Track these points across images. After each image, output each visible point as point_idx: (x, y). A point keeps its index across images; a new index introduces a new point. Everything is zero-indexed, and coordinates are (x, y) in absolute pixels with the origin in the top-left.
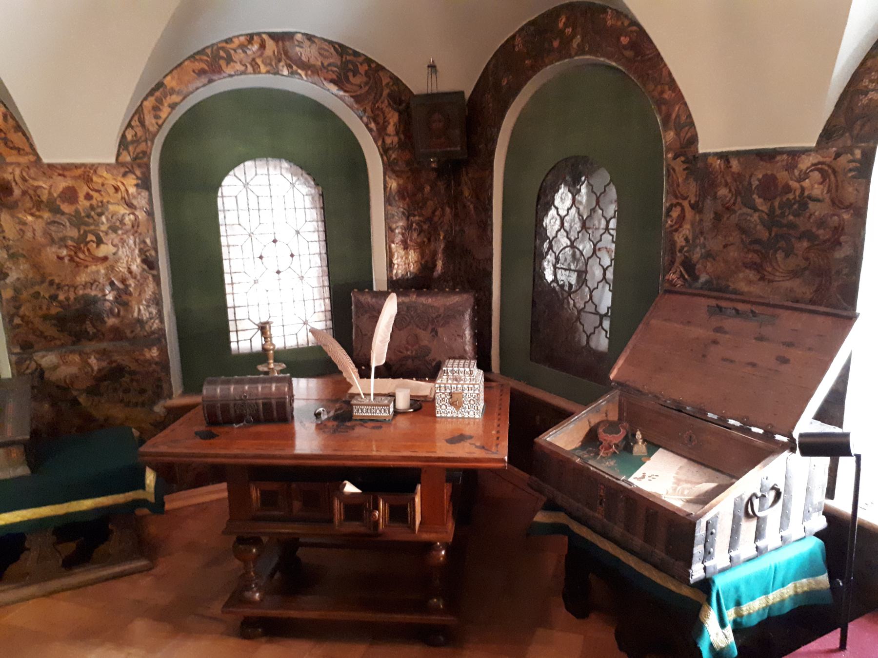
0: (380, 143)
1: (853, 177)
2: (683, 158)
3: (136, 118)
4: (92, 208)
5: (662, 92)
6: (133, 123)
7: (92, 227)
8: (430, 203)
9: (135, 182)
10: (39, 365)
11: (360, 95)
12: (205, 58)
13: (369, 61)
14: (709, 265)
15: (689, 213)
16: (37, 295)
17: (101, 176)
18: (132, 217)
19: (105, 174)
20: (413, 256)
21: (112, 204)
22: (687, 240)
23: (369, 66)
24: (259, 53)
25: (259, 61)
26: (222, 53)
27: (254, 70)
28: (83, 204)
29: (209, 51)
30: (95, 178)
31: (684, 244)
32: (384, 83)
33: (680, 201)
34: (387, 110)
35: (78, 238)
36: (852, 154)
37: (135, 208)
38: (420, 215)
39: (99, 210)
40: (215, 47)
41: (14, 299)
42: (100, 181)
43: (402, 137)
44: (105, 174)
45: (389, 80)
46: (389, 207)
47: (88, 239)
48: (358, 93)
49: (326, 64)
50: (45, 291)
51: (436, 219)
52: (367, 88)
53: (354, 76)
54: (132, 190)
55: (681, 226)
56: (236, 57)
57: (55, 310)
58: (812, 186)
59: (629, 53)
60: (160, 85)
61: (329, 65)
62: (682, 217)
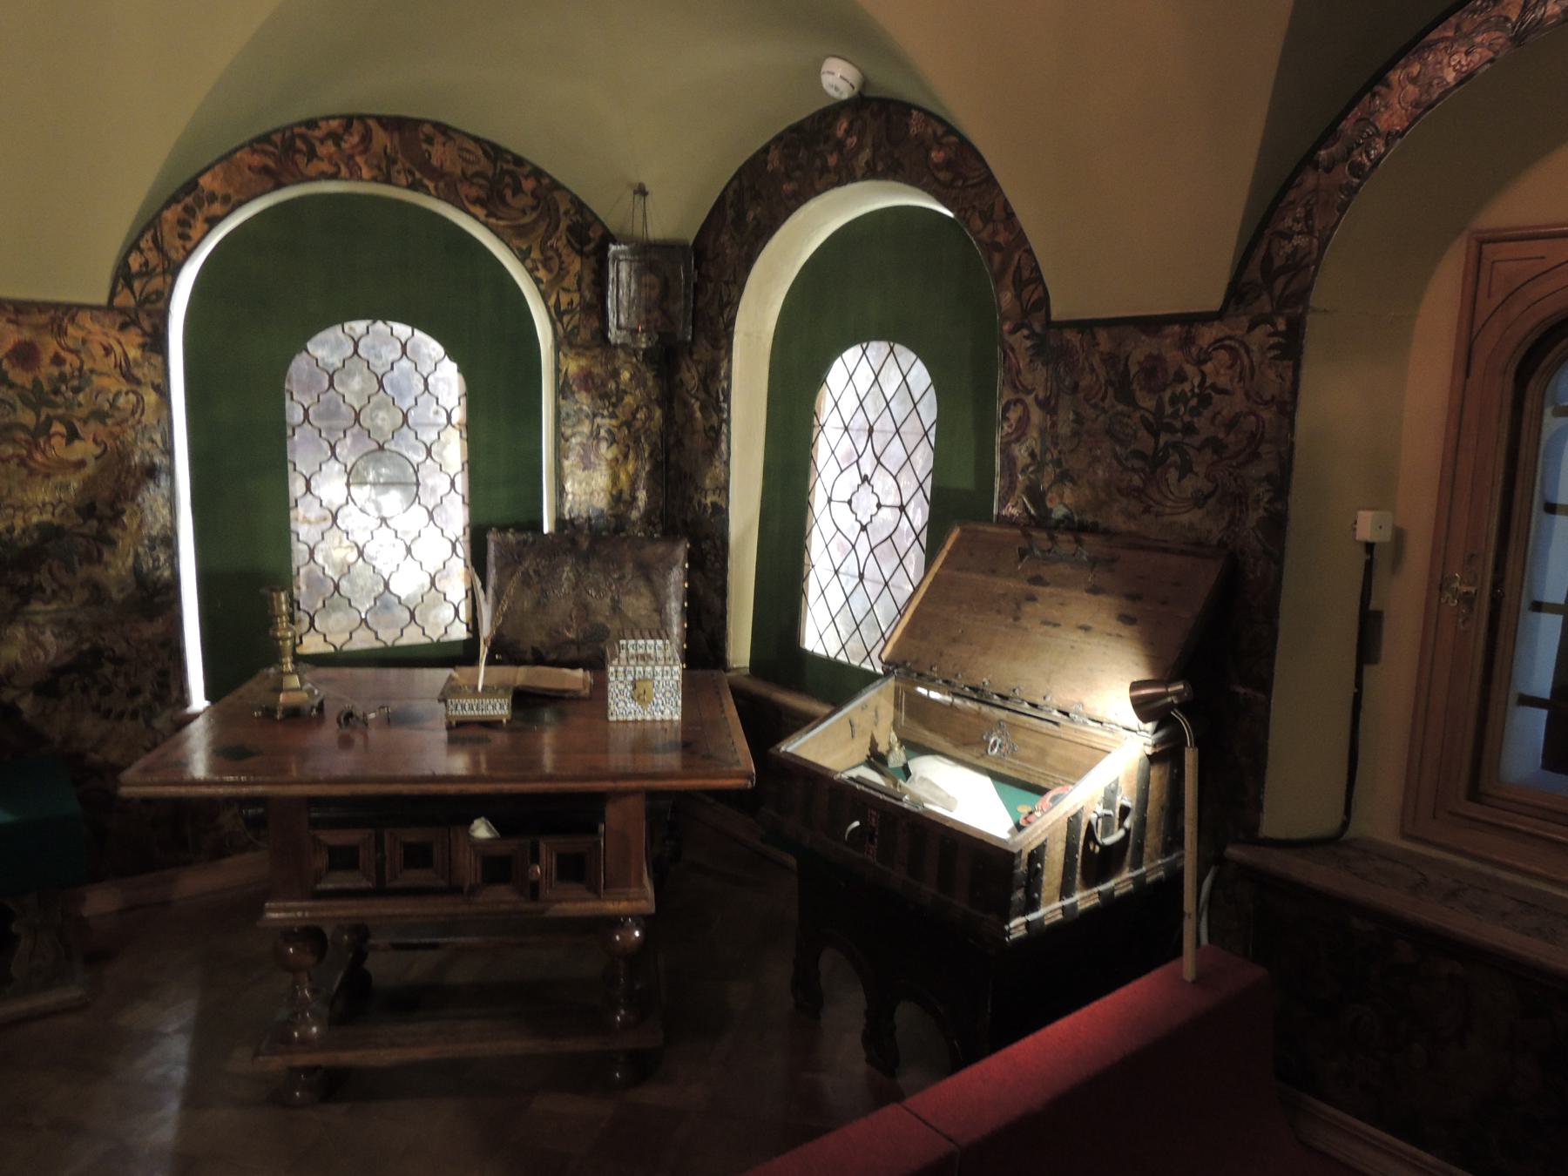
0: (552, 301)
1: (1275, 358)
2: (1025, 332)
3: (148, 236)
4: (63, 378)
5: (995, 233)
6: (143, 244)
7: (60, 411)
8: (628, 399)
9: (139, 340)
11: (523, 226)
12: (271, 149)
13: (538, 173)
14: (1067, 492)
15: (1036, 415)
17: (82, 328)
18: (132, 397)
19: (89, 324)
20: (601, 479)
21: (101, 374)
22: (1032, 454)
23: (538, 181)
24: (361, 148)
25: (359, 160)
26: (299, 144)
27: (351, 174)
28: (47, 370)
29: (277, 138)
30: (71, 330)
31: (1028, 460)
32: (562, 210)
33: (1021, 396)
34: (564, 251)
35: (36, 428)
36: (1274, 325)
37: (138, 382)
38: (613, 416)
39: (75, 383)
40: (288, 134)
42: (80, 334)
43: (587, 294)
44: (89, 324)
46: (562, 402)
47: (53, 430)
49: (469, 173)
51: (638, 424)
52: (534, 215)
54: (134, 353)
55: (1024, 434)
56: (322, 150)
58: (1218, 373)
59: (943, 176)
60: (191, 186)
62: (1024, 421)
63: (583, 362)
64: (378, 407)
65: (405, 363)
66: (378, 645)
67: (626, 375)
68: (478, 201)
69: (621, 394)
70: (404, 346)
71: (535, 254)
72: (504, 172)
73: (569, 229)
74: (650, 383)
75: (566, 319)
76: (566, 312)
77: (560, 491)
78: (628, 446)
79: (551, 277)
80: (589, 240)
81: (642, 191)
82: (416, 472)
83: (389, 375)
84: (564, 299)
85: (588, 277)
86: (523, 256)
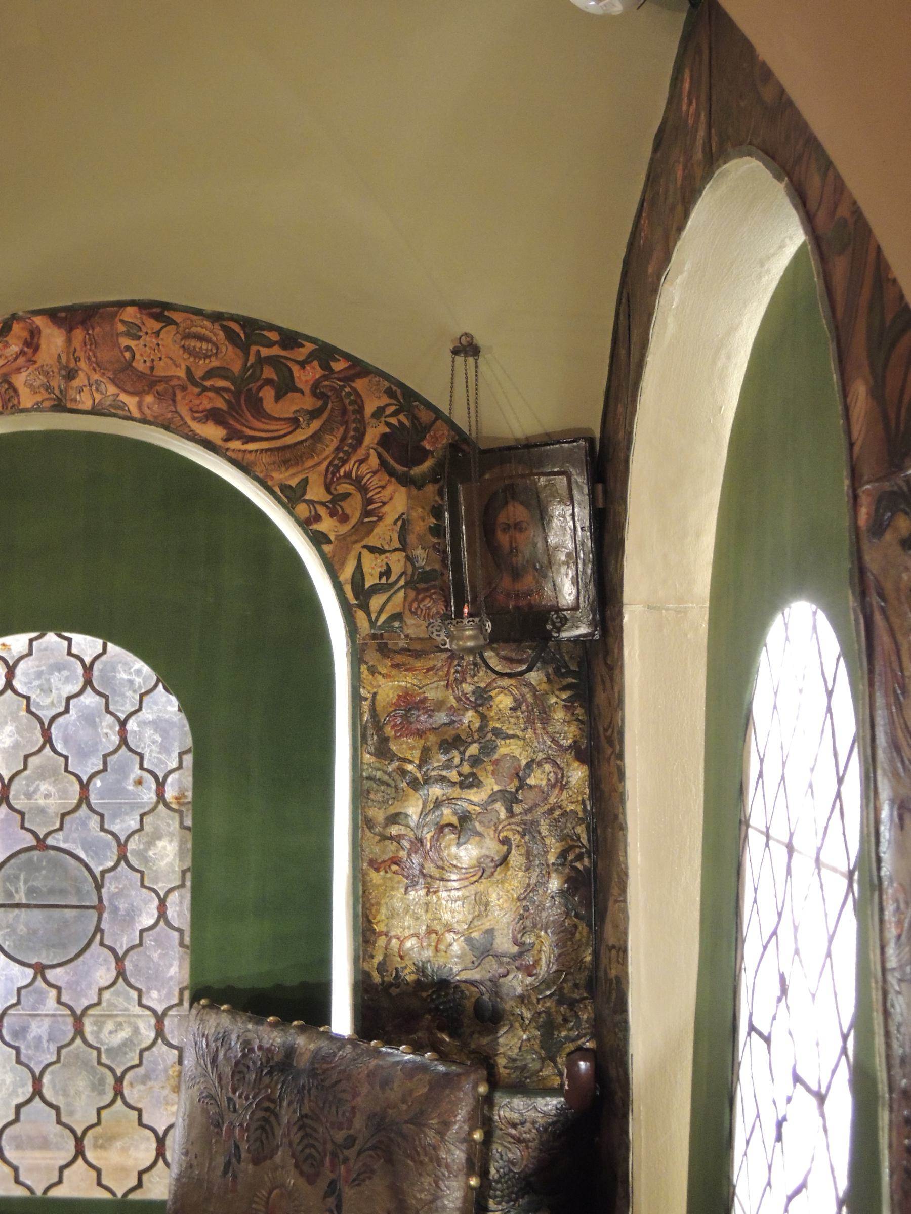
0: (347, 573)
13: (325, 353)
23: (325, 366)
25: (19, 381)
32: (369, 409)
45: (385, 400)
48: (289, 440)
49: (199, 374)
52: (316, 425)
53: (278, 398)
61: (210, 374)
63: (407, 681)
64: (43, 774)
65: (89, 699)
66: (19, 1192)
67: (503, 701)
68: (214, 416)
69: (488, 736)
70: (88, 669)
71: (316, 492)
72: (261, 361)
73: (385, 441)
74: (559, 715)
75: (375, 602)
76: (376, 589)
77: (366, 933)
78: (505, 841)
79: (345, 528)
80: (424, 454)
81: (468, 348)
82: (99, 887)
83: (61, 720)
84: (372, 567)
85: (422, 523)
86: (289, 498)
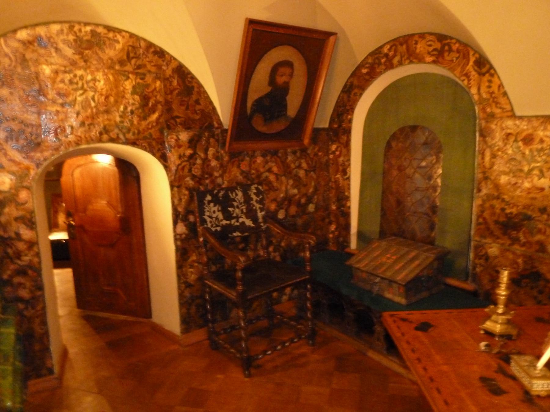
10: (486, 253)
16: (492, 207)
41: (481, 206)
50: (497, 205)
57: (502, 219)
